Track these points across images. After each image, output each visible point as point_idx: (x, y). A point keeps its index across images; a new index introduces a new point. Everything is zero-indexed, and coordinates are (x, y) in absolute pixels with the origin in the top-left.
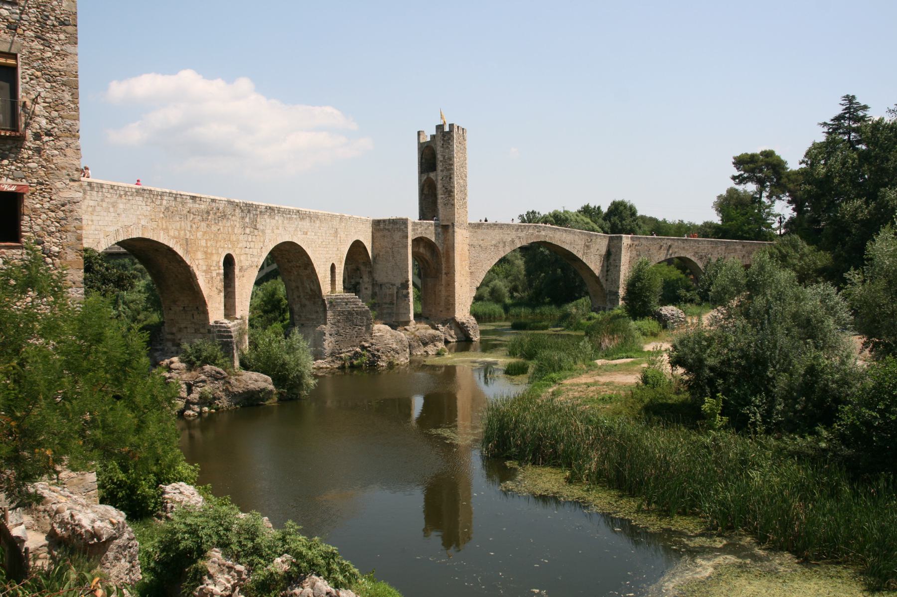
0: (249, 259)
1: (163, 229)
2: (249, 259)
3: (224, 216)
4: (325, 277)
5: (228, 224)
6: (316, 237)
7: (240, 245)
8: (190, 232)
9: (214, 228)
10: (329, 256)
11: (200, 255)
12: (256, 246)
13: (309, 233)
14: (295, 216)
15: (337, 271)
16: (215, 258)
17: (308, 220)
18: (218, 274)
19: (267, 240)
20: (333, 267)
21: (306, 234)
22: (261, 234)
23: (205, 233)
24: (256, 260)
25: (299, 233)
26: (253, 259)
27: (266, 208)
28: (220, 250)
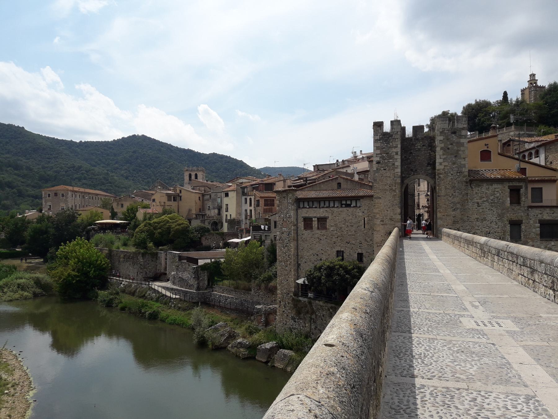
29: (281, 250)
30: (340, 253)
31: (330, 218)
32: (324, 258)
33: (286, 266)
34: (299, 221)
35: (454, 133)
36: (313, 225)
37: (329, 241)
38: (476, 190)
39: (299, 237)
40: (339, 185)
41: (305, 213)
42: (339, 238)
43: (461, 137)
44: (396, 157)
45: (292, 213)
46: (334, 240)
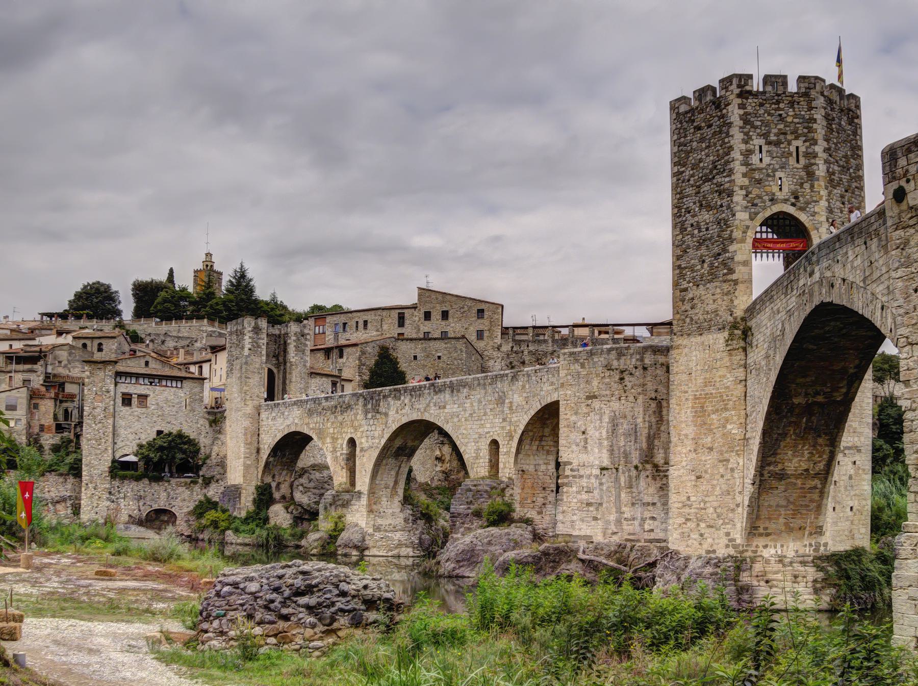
0: (370, 440)
1: (306, 424)
2: (370, 440)
3: (349, 407)
4: (477, 458)
5: (352, 413)
6: (461, 409)
7: (361, 430)
8: (323, 424)
9: (340, 418)
10: (486, 430)
11: (328, 440)
12: (378, 429)
13: (448, 407)
14: (427, 391)
15: (502, 450)
16: (340, 441)
17: (448, 391)
18: (341, 454)
19: (390, 421)
20: (495, 444)
21: (444, 407)
22: (383, 417)
23: (333, 423)
24: (377, 441)
25: (433, 408)
26: (374, 441)
27: (390, 391)
28: (344, 435)
29: (91, 427)
30: (159, 433)
31: (151, 396)
32: (143, 436)
33: (99, 445)
34: (117, 396)
35: (303, 336)
36: (133, 402)
37: (149, 420)
38: (313, 380)
39: (117, 413)
40: (147, 363)
41: (124, 388)
42: (160, 418)
43: (306, 339)
44: (263, 347)
45: (112, 387)
46: (155, 419)
